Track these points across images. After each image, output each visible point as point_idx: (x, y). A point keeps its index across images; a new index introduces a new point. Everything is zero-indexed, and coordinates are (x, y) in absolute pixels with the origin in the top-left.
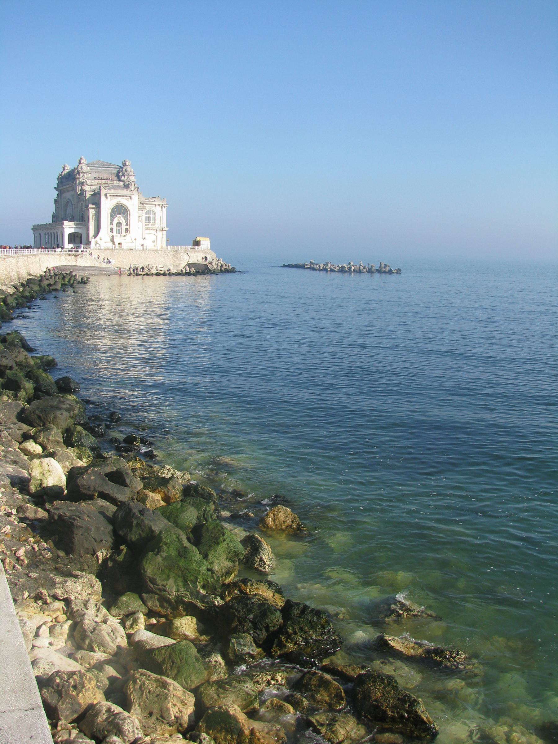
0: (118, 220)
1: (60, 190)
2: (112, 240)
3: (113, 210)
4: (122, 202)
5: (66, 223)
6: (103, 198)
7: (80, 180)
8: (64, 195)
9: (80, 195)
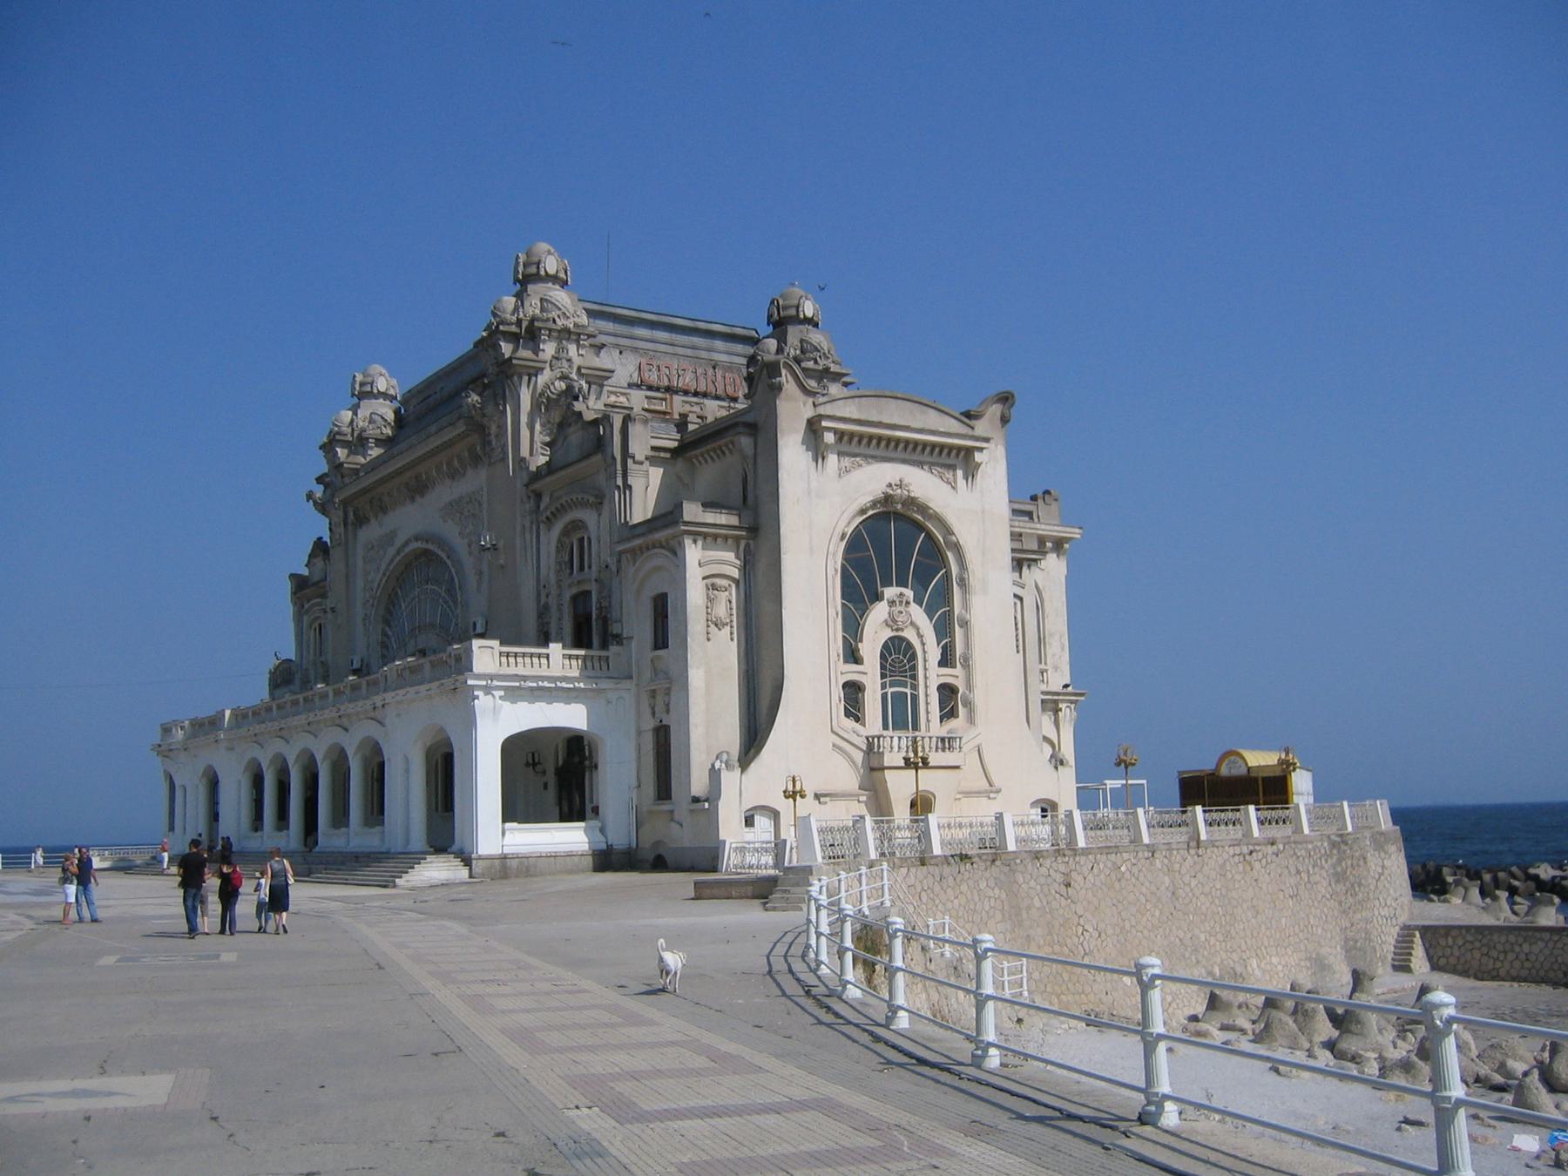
0: (891, 622)
1: (346, 503)
2: (873, 767)
3: (854, 545)
4: (917, 492)
5: (486, 656)
6: (792, 453)
7: (542, 379)
8: (371, 532)
9: (538, 475)
